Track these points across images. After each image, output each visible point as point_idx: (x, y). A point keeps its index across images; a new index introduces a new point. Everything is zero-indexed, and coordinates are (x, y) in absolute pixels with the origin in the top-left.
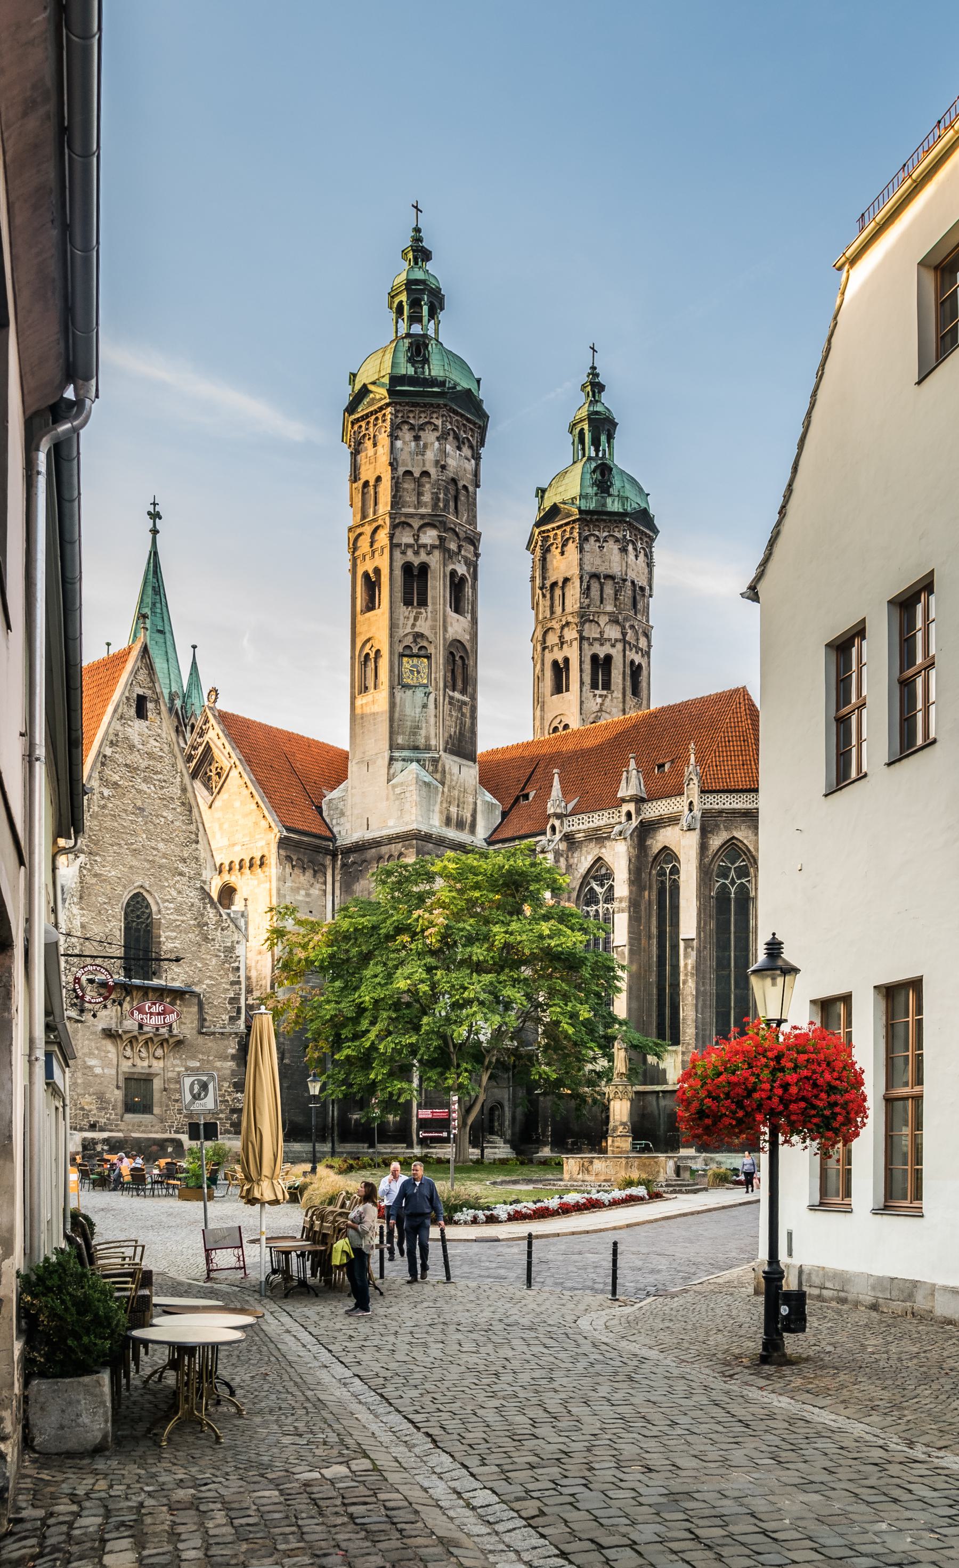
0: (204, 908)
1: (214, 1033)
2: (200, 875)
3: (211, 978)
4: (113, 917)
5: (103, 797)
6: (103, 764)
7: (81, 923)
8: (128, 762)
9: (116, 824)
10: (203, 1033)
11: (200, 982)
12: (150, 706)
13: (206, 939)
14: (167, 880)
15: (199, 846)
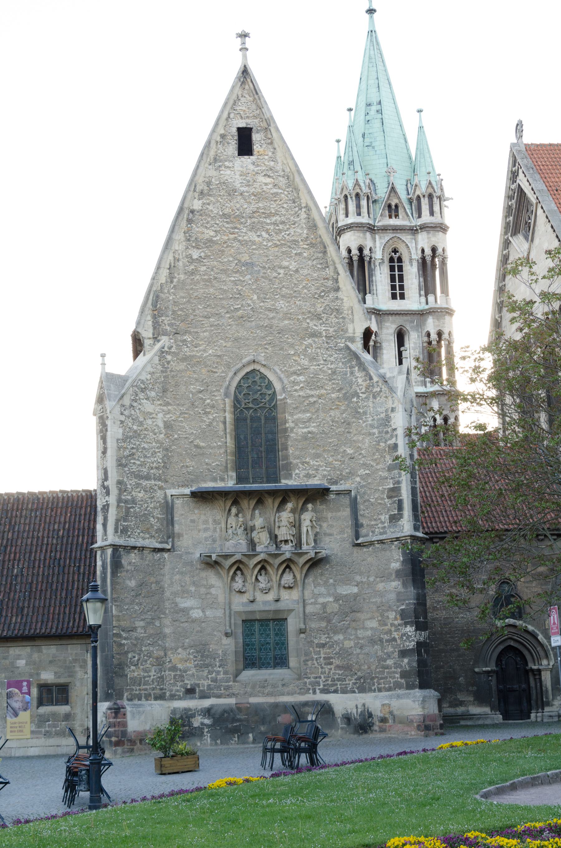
0: (352, 373)
1: (371, 543)
2: (346, 331)
3: (365, 466)
4: (213, 407)
5: (192, 261)
6: (189, 221)
7: (165, 422)
8: (227, 211)
9: (212, 290)
10: (358, 545)
11: (352, 474)
12: (256, 137)
13: (357, 414)
14: (292, 346)
15: (340, 295)
